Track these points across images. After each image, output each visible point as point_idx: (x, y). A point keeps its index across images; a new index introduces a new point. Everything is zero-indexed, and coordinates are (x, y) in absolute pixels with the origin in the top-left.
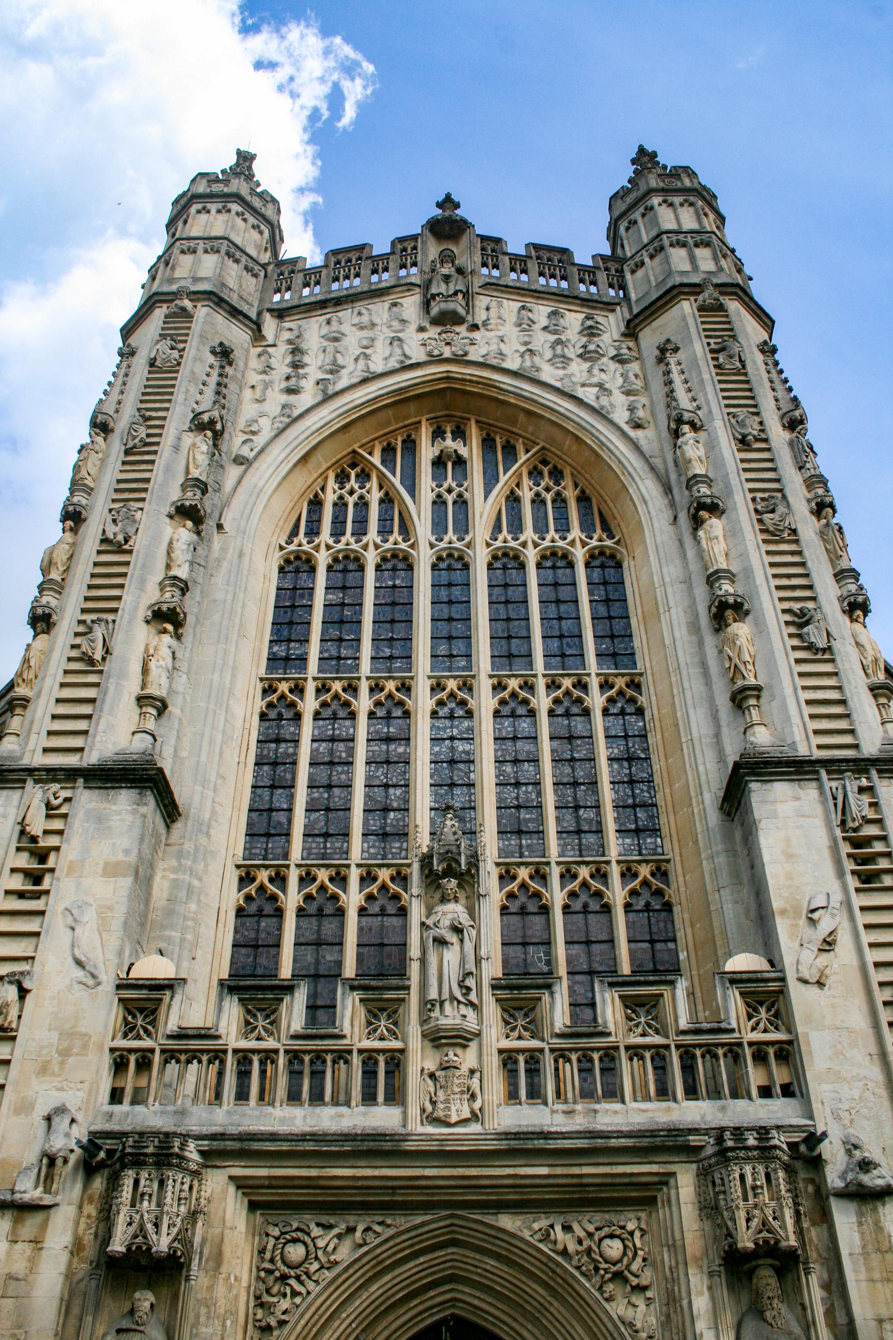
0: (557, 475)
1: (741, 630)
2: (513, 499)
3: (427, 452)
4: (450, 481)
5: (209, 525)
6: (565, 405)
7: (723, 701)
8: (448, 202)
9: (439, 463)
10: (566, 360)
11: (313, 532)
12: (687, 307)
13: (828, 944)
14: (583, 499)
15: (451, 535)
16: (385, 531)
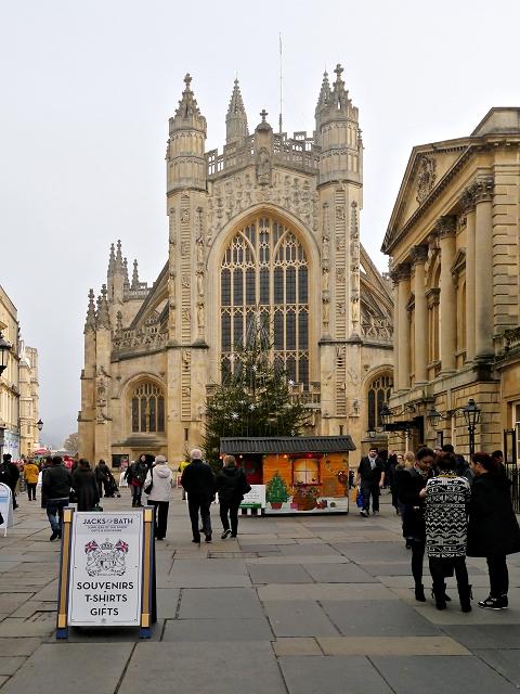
0: (294, 237)
1: (327, 307)
2: (281, 248)
3: (258, 231)
4: (264, 242)
5: (206, 273)
6: (296, 221)
7: (322, 321)
8: (264, 111)
9: (262, 234)
10: (298, 202)
11: (229, 261)
12: (331, 189)
13: (330, 378)
14: (300, 247)
15: (265, 262)
16: (247, 260)
